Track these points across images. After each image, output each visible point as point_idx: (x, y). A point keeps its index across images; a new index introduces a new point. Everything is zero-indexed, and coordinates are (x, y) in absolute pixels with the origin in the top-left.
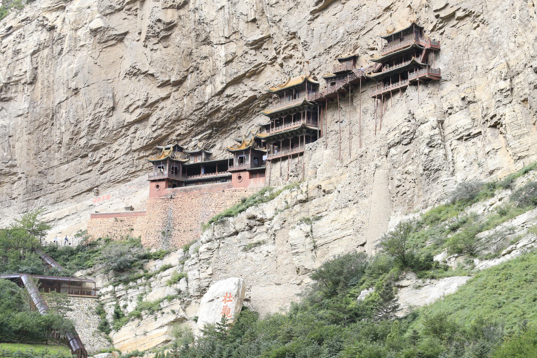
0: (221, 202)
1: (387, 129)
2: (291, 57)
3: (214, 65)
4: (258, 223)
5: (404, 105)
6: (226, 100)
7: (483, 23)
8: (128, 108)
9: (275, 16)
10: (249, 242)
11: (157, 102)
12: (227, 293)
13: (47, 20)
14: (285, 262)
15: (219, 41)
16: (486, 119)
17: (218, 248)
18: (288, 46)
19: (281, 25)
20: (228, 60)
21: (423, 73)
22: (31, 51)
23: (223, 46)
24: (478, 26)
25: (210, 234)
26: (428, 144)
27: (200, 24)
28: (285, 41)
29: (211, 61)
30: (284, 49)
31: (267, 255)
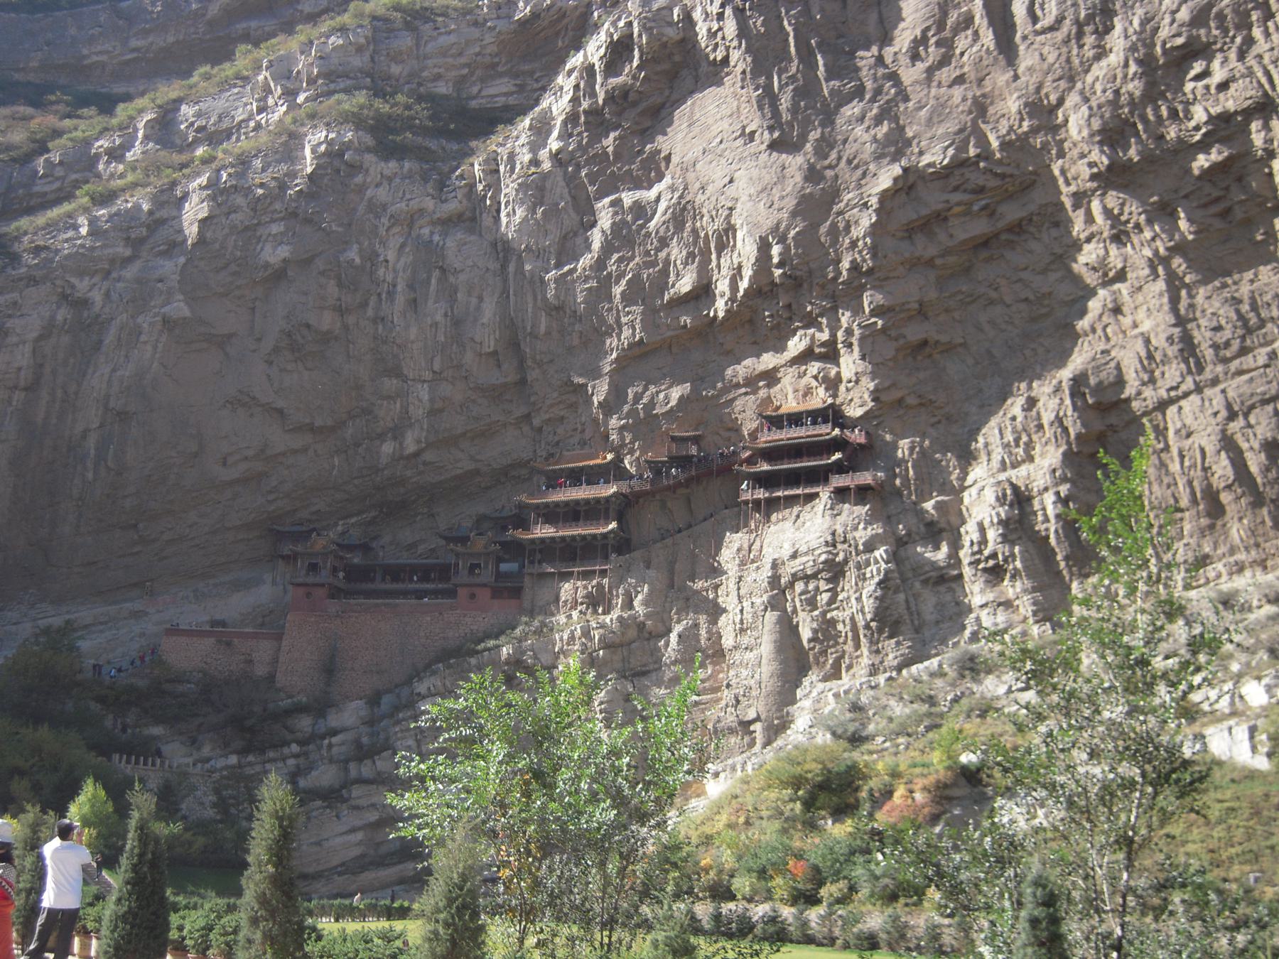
1: (786, 552)
2: (562, 418)
5: (819, 520)
7: (947, 419)
8: (225, 459)
11: (284, 454)
13: (73, 287)
16: (978, 557)
20: (436, 406)
21: (865, 478)
22: (35, 334)
24: (939, 422)
26: (879, 584)
27: (385, 342)
28: (555, 395)
29: (398, 405)
30: (552, 406)
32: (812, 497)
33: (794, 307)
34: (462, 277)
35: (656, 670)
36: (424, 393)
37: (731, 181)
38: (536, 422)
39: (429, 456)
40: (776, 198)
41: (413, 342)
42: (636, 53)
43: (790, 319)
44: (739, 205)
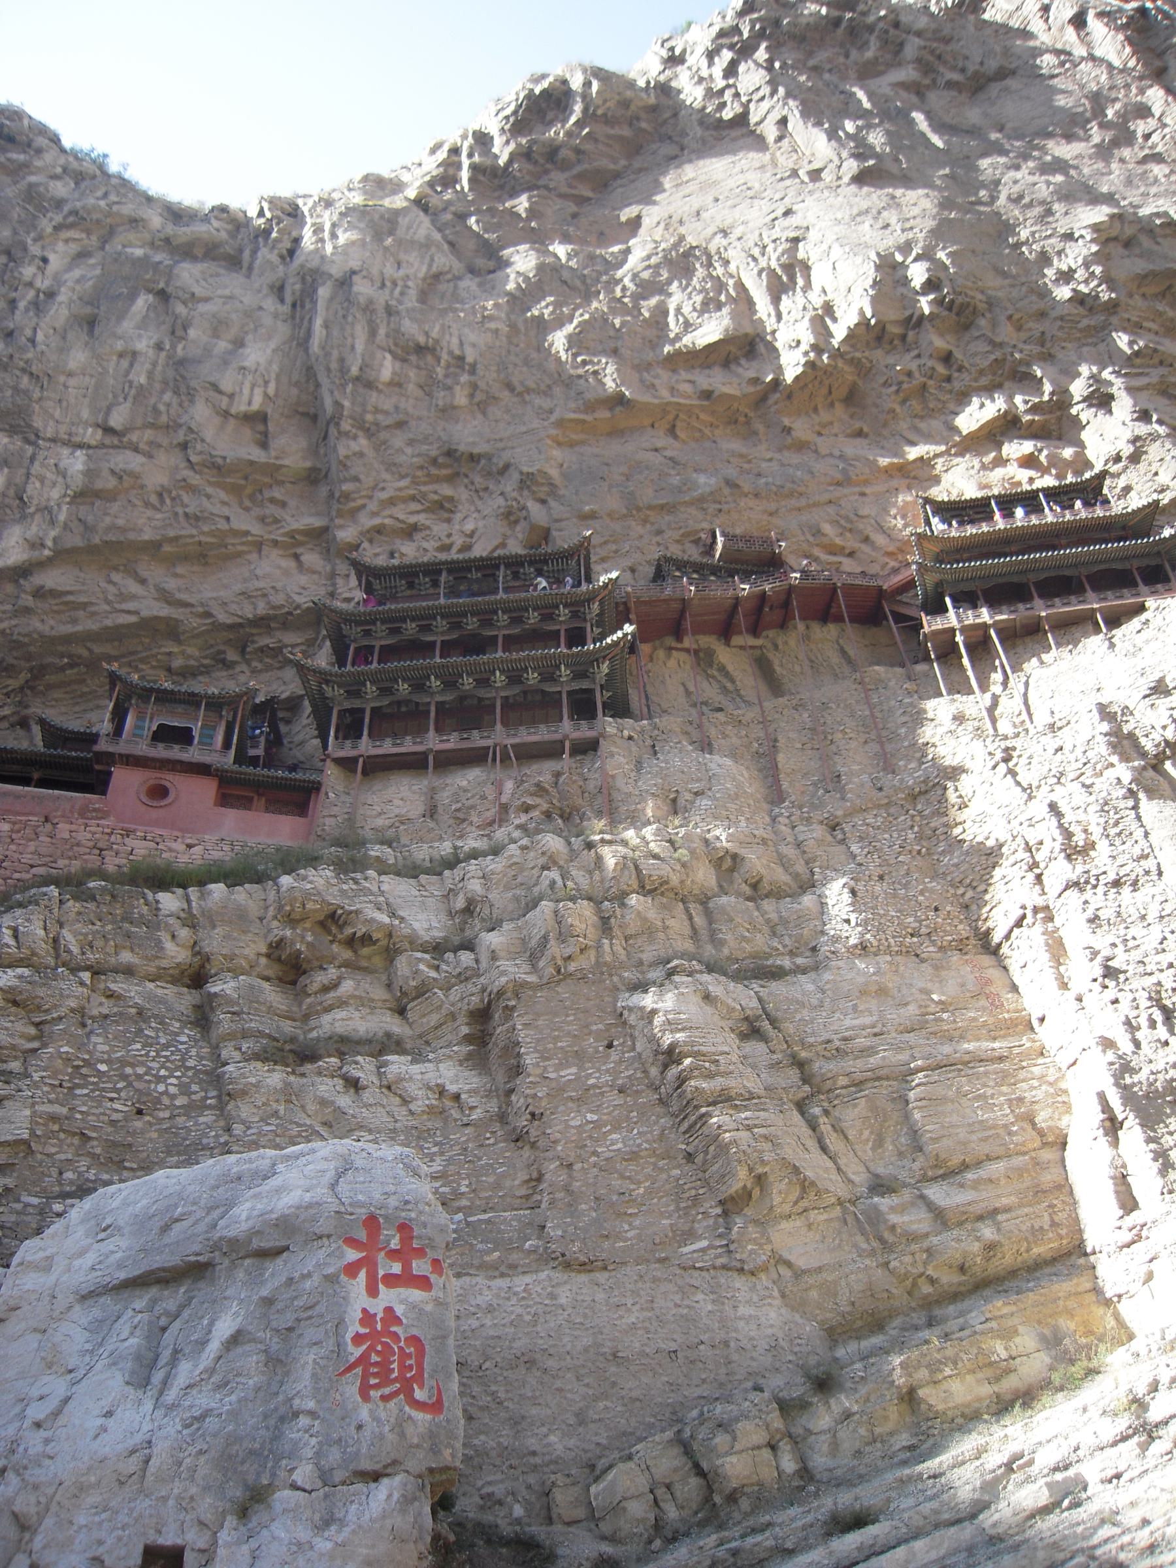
0: (27, 858)
2: (410, 531)
3: (11, 493)
4: (347, 954)
6: (20, 602)
9: (377, 410)
10: (288, 1027)
12: (372, 1222)
14: (617, 1141)
15: (70, 434)
17: (81, 1011)
18: (413, 498)
19: (398, 440)
20: (99, 485)
23: (78, 453)
25: (35, 930)
30: (391, 502)
31: (431, 1111)
32: (1114, 621)
33: (958, 354)
34: (203, 308)
35: (804, 971)
36: (76, 463)
37: (788, 213)
38: (346, 534)
39: (51, 579)
40: (893, 220)
41: (70, 375)
42: (578, 108)
43: (949, 379)
44: (812, 235)
